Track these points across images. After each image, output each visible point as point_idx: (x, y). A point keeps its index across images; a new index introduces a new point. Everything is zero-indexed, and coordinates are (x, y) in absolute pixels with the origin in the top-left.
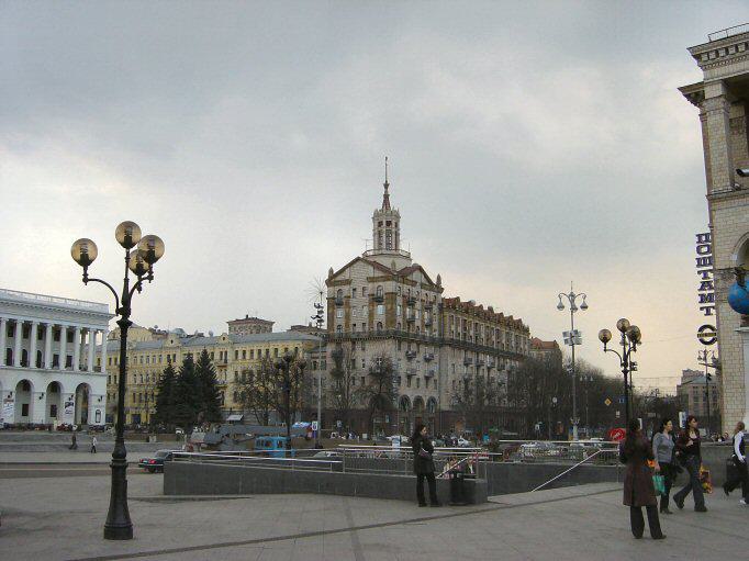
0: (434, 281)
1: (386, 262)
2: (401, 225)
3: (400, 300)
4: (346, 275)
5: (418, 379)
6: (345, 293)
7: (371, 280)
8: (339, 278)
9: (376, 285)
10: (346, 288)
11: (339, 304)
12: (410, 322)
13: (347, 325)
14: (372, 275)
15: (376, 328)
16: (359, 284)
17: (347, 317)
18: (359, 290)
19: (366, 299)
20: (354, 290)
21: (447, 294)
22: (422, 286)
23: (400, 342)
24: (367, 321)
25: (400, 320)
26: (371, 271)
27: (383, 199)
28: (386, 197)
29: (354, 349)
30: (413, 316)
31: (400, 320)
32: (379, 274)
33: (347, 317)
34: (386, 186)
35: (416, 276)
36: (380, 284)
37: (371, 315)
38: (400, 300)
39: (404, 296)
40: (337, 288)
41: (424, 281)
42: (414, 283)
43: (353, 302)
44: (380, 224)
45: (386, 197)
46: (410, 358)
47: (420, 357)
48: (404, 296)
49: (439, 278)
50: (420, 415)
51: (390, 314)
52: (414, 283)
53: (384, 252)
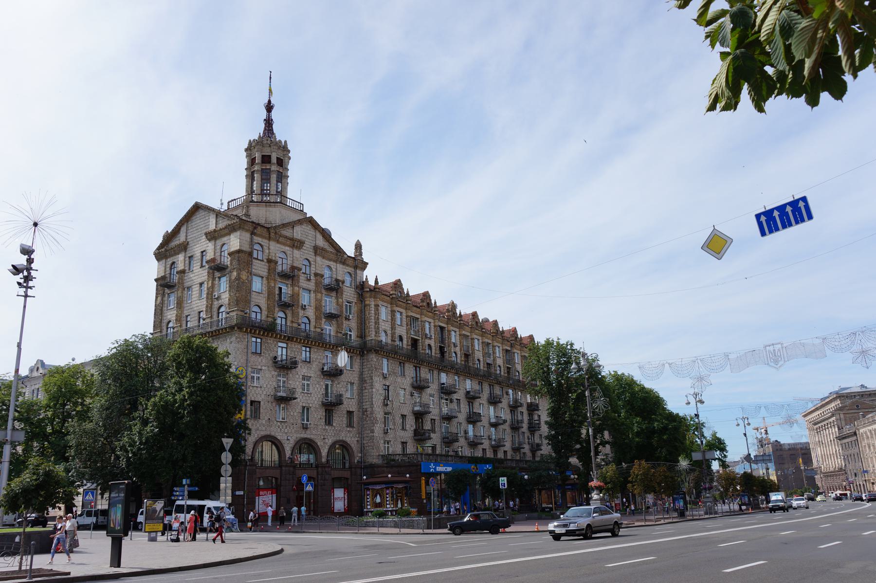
0: (350, 251)
3: (260, 268)
5: (306, 409)
6: (180, 266)
10: (180, 260)
11: (170, 286)
13: (178, 319)
14: (212, 227)
20: (191, 257)
21: (370, 275)
22: (317, 250)
27: (262, 126)
28: (269, 123)
30: (295, 297)
34: (269, 107)
38: (260, 268)
39: (269, 261)
40: (170, 261)
41: (321, 242)
42: (297, 244)
44: (252, 162)
45: (269, 123)
46: (285, 367)
48: (269, 261)
49: (358, 247)
52: (297, 244)
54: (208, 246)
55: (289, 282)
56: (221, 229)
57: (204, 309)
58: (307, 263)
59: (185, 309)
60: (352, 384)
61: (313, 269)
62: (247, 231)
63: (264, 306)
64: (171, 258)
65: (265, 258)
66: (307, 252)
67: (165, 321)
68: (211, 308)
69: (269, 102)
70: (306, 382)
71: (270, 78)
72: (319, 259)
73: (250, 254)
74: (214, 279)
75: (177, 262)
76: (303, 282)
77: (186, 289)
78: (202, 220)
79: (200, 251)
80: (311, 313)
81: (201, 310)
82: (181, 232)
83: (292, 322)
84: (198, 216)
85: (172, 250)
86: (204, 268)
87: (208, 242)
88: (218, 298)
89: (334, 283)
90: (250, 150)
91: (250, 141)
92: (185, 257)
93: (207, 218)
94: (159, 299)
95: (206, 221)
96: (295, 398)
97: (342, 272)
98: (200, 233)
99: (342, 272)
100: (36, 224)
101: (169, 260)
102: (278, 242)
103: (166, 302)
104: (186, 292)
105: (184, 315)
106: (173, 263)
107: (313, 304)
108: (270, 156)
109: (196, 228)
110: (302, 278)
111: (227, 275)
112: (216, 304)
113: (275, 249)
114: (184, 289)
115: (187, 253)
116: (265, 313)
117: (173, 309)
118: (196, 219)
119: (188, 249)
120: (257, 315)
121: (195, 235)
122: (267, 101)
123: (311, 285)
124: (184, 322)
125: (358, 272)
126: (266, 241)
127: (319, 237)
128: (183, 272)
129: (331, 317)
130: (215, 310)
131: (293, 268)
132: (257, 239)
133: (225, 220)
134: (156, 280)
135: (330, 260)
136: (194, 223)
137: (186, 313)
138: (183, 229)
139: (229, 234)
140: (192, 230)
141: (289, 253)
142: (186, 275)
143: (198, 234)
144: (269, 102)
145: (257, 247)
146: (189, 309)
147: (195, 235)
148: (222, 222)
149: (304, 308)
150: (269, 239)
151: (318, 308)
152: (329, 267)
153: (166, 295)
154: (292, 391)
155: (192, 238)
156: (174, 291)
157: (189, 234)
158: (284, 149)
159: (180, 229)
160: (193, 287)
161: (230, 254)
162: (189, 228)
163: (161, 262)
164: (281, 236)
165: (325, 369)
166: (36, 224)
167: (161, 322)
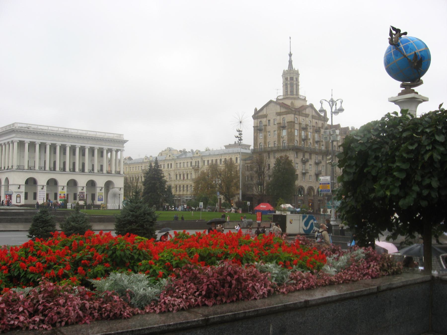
1: (288, 102)
2: (301, 79)
3: (297, 126)
4: (264, 112)
6: (264, 123)
7: (279, 114)
8: (261, 114)
9: (282, 117)
10: (264, 121)
11: (260, 130)
12: (305, 140)
13: (265, 143)
15: (282, 144)
16: (272, 116)
17: (265, 137)
18: (272, 121)
19: (276, 127)
20: (269, 121)
23: (297, 153)
24: (277, 140)
25: (297, 138)
26: (278, 109)
27: (288, 63)
28: (290, 62)
29: (269, 158)
30: (307, 136)
31: (297, 138)
32: (283, 110)
33: (265, 137)
34: (290, 55)
35: (308, 111)
36: (284, 116)
37: (279, 136)
38: (297, 126)
39: (300, 124)
40: (259, 120)
41: (314, 113)
42: (307, 116)
43: (268, 128)
44: (286, 79)
45: (290, 62)
46: (304, 162)
47: (312, 162)
50: (312, 198)
51: (291, 136)
52: (307, 116)
53: (289, 96)
55: (305, 130)
56: (283, 112)
57: (277, 141)
58: (310, 122)
60: (324, 166)
61: (312, 124)
62: (293, 114)
63: (298, 141)
65: (298, 122)
66: (310, 118)
67: (259, 143)
68: (280, 141)
69: (290, 52)
70: (310, 166)
72: (313, 120)
73: (294, 122)
74: (280, 130)
76: (309, 130)
80: (311, 141)
83: (306, 145)
88: (283, 138)
89: (318, 128)
90: (285, 74)
91: (284, 70)
92: (266, 120)
94: (255, 134)
96: (308, 173)
97: (320, 123)
99: (320, 123)
100: (241, 122)
102: (302, 116)
106: (261, 121)
107: (312, 138)
108: (293, 78)
110: (309, 128)
112: (282, 139)
113: (301, 119)
115: (267, 118)
116: (299, 143)
120: (296, 144)
123: (311, 130)
125: (326, 123)
126: (298, 116)
127: (314, 111)
128: (266, 125)
129: (317, 142)
130: (281, 141)
131: (307, 125)
132: (296, 116)
134: (253, 127)
135: (316, 119)
137: (268, 141)
138: (265, 109)
139: (286, 114)
141: (305, 119)
144: (290, 52)
145: (296, 119)
149: (309, 139)
150: (299, 115)
151: (314, 139)
152: (316, 123)
154: (307, 170)
158: (297, 73)
161: (287, 122)
163: (255, 120)
164: (303, 114)
165: (317, 161)
166: (241, 122)
167: (257, 143)
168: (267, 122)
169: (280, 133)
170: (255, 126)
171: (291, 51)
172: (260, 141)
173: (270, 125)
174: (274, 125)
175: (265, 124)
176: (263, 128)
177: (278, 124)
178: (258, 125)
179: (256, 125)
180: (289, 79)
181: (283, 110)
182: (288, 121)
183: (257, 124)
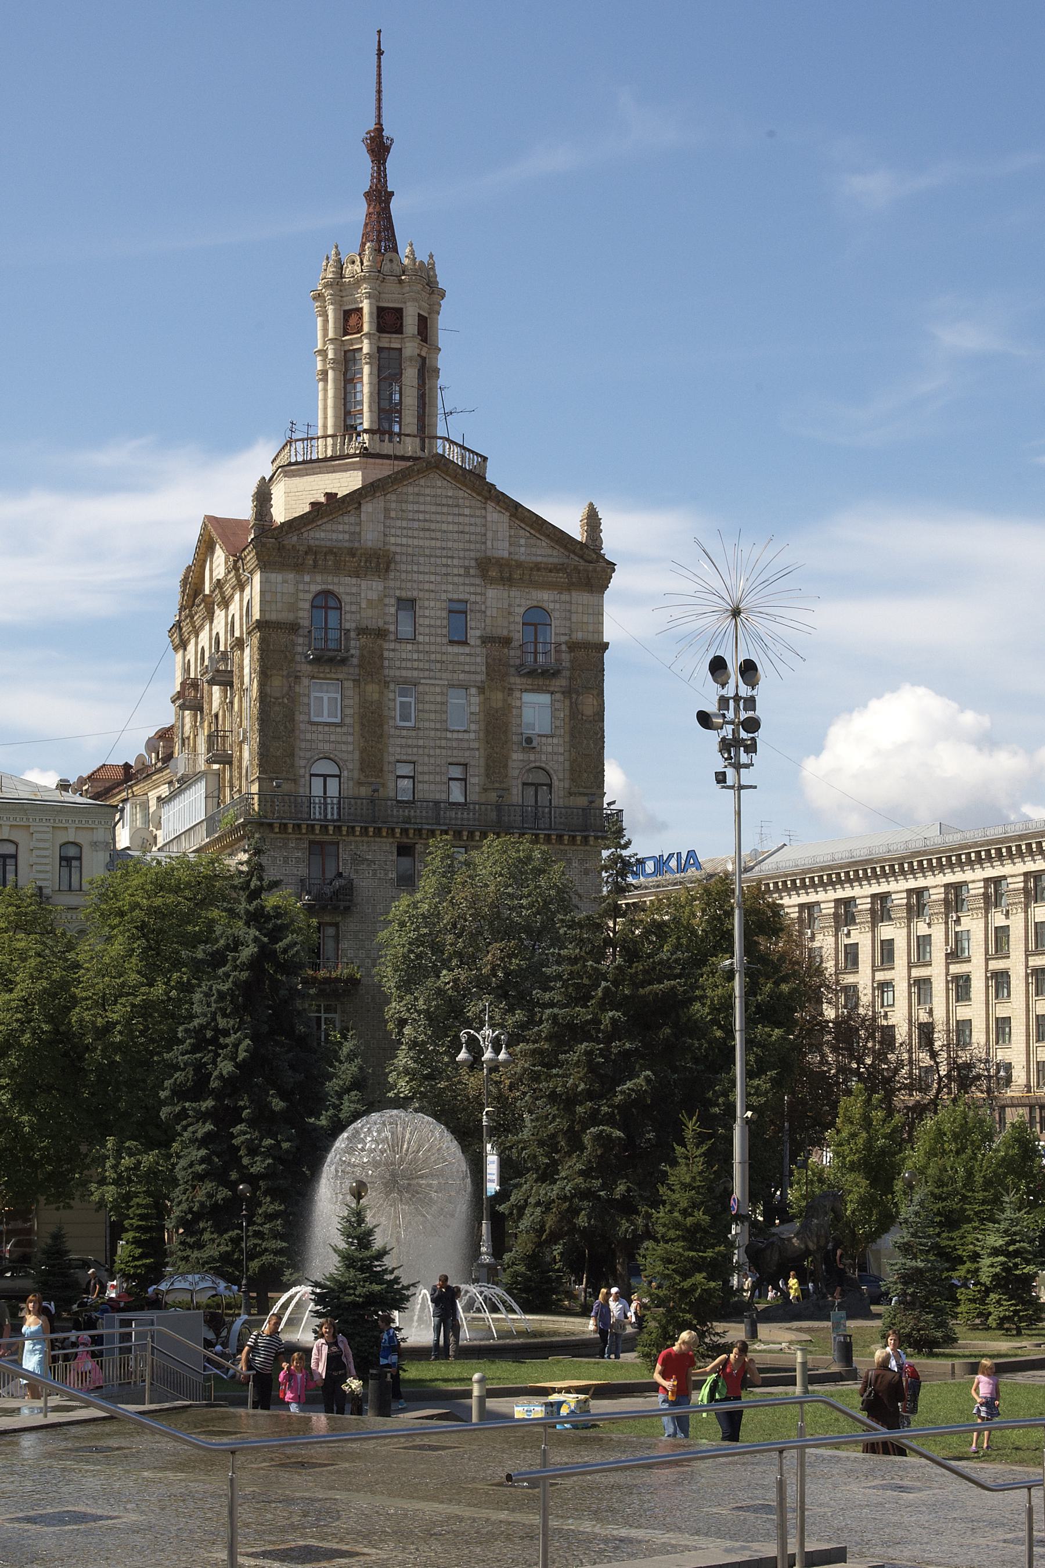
9: (521, 600)
14: (501, 549)
20: (408, 604)
36: (545, 597)
40: (315, 584)
54: (475, 594)
56: (537, 567)
59: (392, 741)
64: (319, 578)
69: (379, 129)
71: (380, 53)
75: (346, 599)
77: (392, 686)
78: (445, 510)
79: (444, 596)
81: (462, 761)
82: (363, 517)
84: (428, 491)
85: (331, 557)
86: (467, 650)
87: (478, 581)
93: (467, 511)
94: (277, 682)
95: (461, 519)
98: (438, 544)
100: (736, 613)
101: (307, 578)
103: (305, 700)
104: (391, 696)
105: (392, 759)
106: (327, 594)
109: (427, 525)
111: (558, 696)
114: (387, 684)
117: (338, 729)
118: (421, 499)
119: (392, 575)
121: (416, 542)
122: (372, 127)
124: (392, 777)
128: (381, 634)
133: (533, 541)
136: (410, 507)
137: (394, 750)
139: (569, 587)
140: (404, 524)
142: (386, 645)
143: (433, 543)
146: (409, 746)
147: (416, 542)
148: (526, 546)
153: (305, 681)
155: (408, 546)
156: (340, 676)
157: (393, 531)
159: (360, 504)
160: (421, 688)
161: (574, 647)
162: (393, 514)
163: (276, 577)
168: (393, 610)
169: (507, 708)
170: (273, 617)
171: (384, 122)
172: (327, 747)
173: (413, 640)
174: (452, 642)
175: (372, 624)
176: (355, 647)
177: (486, 640)
178: (304, 617)
179: (285, 616)
180: (410, 324)
181: (544, 552)
182: (579, 636)
183: (293, 607)
